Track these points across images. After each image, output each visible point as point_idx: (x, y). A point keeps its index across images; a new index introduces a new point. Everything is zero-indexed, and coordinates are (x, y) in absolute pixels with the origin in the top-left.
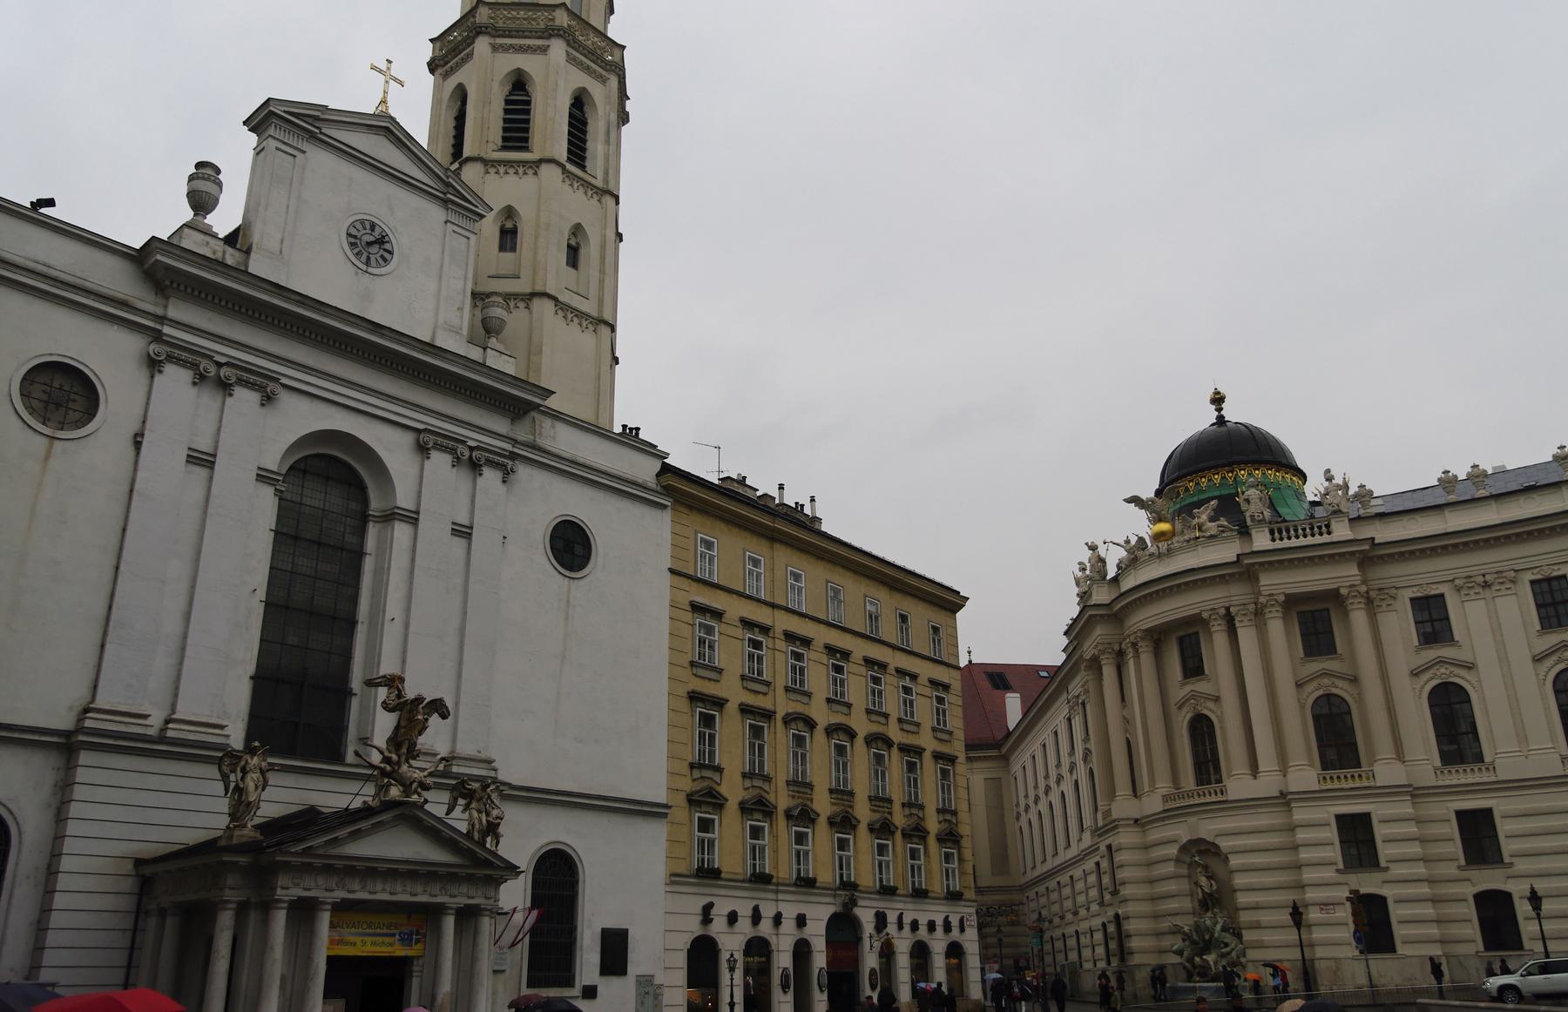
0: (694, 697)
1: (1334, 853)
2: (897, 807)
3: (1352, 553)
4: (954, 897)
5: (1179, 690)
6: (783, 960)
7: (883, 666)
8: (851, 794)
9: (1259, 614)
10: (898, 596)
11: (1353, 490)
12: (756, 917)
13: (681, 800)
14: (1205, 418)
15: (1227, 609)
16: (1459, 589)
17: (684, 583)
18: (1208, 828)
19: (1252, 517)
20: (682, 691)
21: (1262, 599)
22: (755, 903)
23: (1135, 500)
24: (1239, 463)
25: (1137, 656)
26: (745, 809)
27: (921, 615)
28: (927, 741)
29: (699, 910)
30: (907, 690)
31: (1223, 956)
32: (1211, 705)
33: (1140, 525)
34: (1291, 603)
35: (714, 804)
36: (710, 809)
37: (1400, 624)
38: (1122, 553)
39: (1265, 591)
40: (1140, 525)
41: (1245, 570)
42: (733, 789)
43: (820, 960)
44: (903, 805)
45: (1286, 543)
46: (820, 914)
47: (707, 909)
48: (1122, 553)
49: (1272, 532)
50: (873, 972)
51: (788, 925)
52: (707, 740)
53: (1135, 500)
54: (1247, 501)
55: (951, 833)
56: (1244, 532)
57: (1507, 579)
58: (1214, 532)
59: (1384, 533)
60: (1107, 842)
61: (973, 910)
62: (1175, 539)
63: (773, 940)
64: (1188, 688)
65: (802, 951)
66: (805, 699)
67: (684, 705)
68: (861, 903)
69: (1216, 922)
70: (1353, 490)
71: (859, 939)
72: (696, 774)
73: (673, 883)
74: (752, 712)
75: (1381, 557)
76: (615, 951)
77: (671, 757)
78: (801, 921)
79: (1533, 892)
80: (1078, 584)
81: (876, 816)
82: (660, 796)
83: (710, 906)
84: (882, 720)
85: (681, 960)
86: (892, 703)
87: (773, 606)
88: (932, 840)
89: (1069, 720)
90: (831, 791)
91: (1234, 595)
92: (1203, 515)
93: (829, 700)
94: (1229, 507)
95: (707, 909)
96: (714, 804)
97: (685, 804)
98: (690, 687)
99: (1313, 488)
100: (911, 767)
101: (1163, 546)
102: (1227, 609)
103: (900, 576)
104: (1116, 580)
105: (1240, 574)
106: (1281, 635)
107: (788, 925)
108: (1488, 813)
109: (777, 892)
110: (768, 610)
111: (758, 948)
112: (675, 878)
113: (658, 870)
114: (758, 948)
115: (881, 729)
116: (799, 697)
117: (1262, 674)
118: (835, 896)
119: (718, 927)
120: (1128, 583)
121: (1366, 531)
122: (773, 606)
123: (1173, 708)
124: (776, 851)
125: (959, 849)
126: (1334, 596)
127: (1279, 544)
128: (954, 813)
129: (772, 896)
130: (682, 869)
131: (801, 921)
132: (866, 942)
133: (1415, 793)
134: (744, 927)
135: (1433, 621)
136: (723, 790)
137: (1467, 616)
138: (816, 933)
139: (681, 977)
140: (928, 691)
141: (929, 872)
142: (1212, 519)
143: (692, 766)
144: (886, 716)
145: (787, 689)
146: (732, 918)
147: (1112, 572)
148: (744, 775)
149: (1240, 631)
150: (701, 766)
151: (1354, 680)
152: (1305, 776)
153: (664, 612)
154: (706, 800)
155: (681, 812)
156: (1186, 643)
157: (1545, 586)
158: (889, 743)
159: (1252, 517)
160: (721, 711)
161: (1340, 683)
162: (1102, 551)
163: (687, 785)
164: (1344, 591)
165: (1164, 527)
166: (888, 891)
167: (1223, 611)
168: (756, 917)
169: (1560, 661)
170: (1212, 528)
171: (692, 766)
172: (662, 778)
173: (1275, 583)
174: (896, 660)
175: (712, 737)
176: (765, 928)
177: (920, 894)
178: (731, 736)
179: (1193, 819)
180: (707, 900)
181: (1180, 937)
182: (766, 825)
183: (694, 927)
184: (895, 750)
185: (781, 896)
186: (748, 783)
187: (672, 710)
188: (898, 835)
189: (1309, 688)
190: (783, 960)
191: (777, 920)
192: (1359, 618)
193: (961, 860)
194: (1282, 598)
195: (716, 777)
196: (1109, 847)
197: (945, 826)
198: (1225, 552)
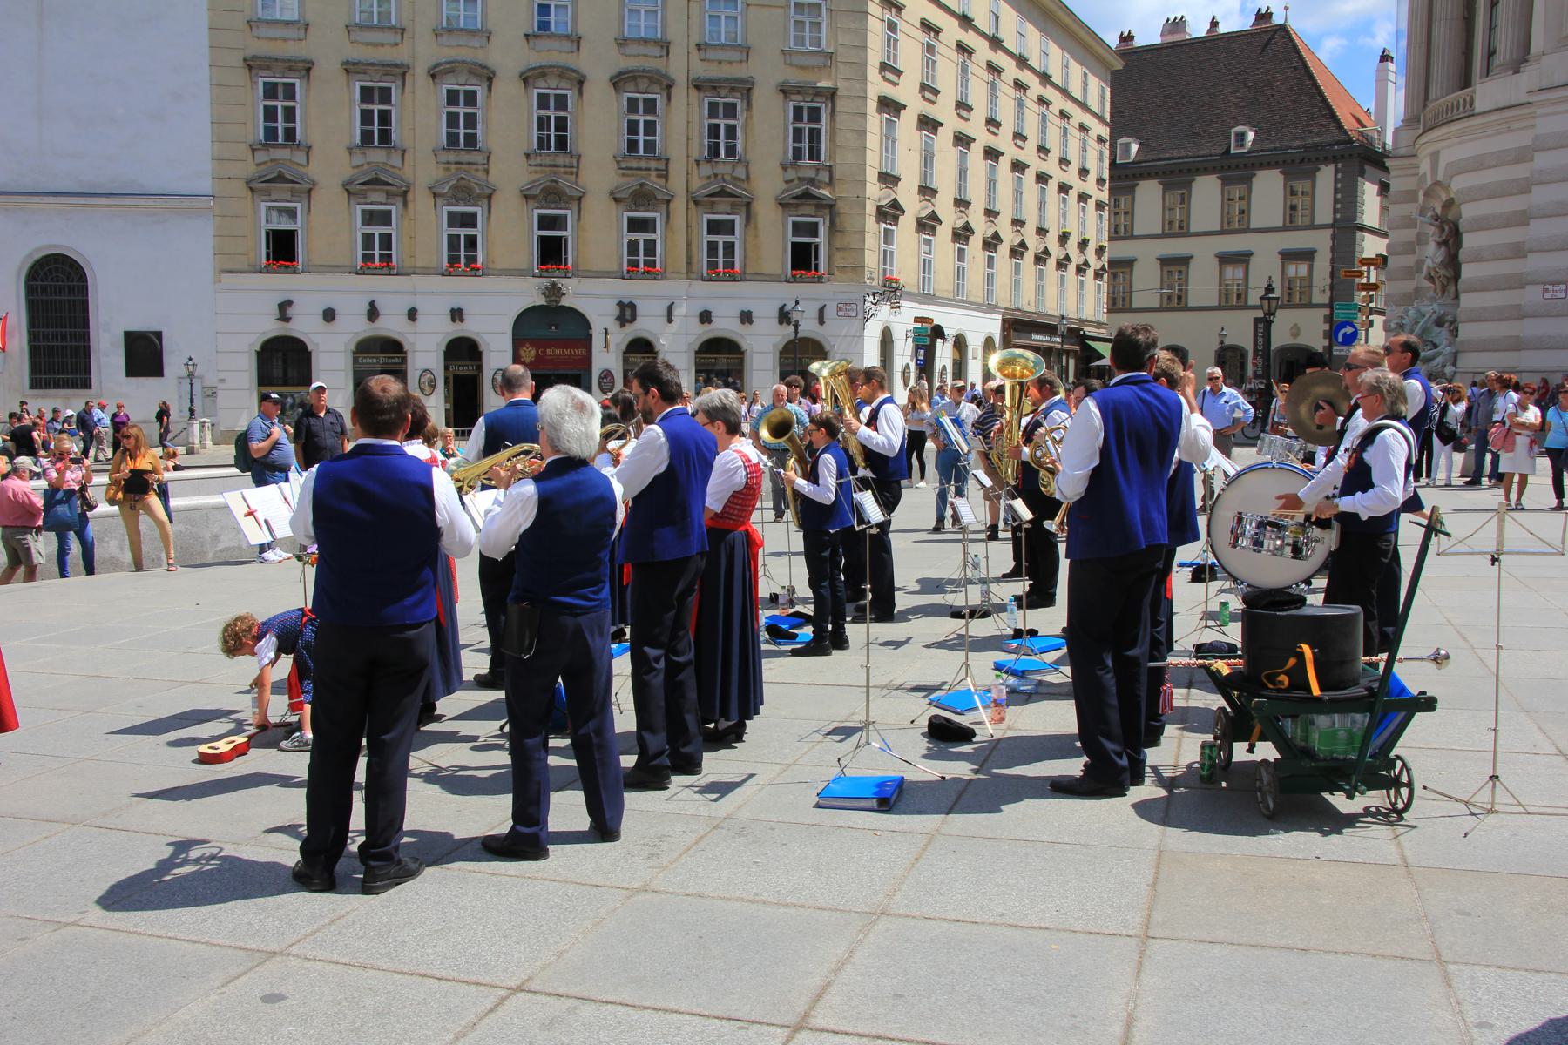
0: (252, 65)
12: (373, 313)
13: (240, 188)
20: (236, 59)
29: (276, 310)
65: (463, 352)
72: (262, 156)
77: (218, 139)
83: (290, 303)
98: (250, 53)
119: (305, 326)
134: (353, 327)
136: (315, 170)
145: (437, 33)
146: (329, 315)
150: (265, 146)
163: (249, 169)
168: (373, 313)
176: (391, 325)
183: (271, 327)
187: (217, 85)
190: (426, 355)
193: (833, 228)
195: (300, 157)
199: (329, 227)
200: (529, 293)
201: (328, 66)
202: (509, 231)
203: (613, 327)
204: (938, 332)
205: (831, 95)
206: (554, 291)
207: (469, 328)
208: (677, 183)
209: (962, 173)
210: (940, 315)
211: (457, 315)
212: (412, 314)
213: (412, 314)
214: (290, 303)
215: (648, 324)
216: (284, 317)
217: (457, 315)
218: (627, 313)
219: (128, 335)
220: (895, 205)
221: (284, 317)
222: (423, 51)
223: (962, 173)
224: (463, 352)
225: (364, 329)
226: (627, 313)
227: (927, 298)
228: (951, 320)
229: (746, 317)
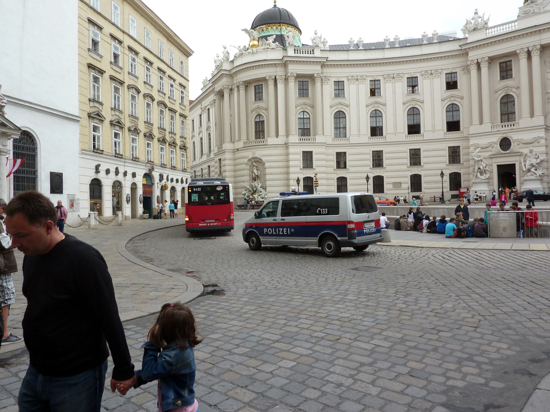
0: (90, 66)
1: (300, 163)
2: (167, 133)
3: (320, 62)
4: (184, 170)
5: (253, 105)
6: (127, 191)
7: (164, 73)
8: (152, 125)
9: (286, 79)
10: (170, 44)
11: (322, 40)
14: (270, 6)
15: (275, 77)
16: (348, 80)
18: (259, 153)
19: (289, 43)
20: (85, 62)
21: (289, 74)
22: (117, 166)
23: (245, 30)
24: (283, 23)
25: (238, 90)
26: (112, 124)
27: (177, 55)
28: (177, 107)
30: (172, 86)
31: (260, 195)
32: (264, 111)
33: (245, 40)
34: (298, 76)
35: (100, 120)
36: (98, 122)
37: (329, 89)
38: (237, 51)
39: (290, 71)
40: (245, 40)
41: (284, 64)
43: (140, 191)
44: (169, 133)
45: (299, 55)
46: (141, 172)
47: (97, 167)
48: (237, 51)
49: (295, 50)
50: (158, 196)
51: (129, 176)
52: (96, 89)
53: (245, 30)
54: (288, 37)
55: (184, 146)
56: (285, 49)
57: (363, 78)
58: (274, 47)
59: (333, 56)
60: (219, 158)
61: (190, 176)
62: (259, 48)
63: (123, 182)
64: (256, 105)
65: (134, 187)
66: (136, 80)
68: (155, 170)
69: (258, 184)
70: (322, 40)
71: (153, 184)
72: (92, 104)
73: (83, 153)
74: (115, 80)
75: (327, 65)
77: (81, 94)
78: (134, 175)
79: (367, 176)
80: (215, 62)
81: (161, 136)
82: (76, 112)
83: (99, 165)
84: (163, 96)
85: (87, 189)
86: (167, 90)
87: (124, 32)
88: (178, 147)
89: (200, 115)
90: (145, 122)
91: (279, 72)
92: (271, 40)
93: (145, 82)
94: (280, 39)
95: (97, 167)
96: (100, 120)
97: (87, 118)
99: (306, 39)
100: (172, 118)
101: (255, 49)
102: (275, 77)
103: (172, 35)
104: (232, 62)
105: (282, 64)
106: (293, 86)
107: (129, 176)
108: (345, 153)
109: (125, 162)
110: (121, 33)
111: (117, 186)
112: (83, 151)
114: (117, 186)
115: (163, 100)
116: (133, 78)
117: (284, 101)
118: (146, 166)
119: (102, 176)
120: (237, 63)
121: (325, 55)
122: (124, 32)
123: (250, 111)
124: (124, 145)
125: (186, 152)
126: (312, 77)
127: (296, 55)
128: (185, 138)
129: (123, 164)
131: (134, 175)
132: (156, 185)
133: (327, 146)
134: (112, 177)
135: (339, 88)
136: (103, 113)
137: (350, 89)
138: (140, 181)
139: (87, 195)
140: (178, 87)
141: (176, 160)
142: (273, 42)
143: (90, 100)
144: (165, 94)
146: (108, 172)
147: (231, 58)
148: (112, 109)
149: (278, 85)
150: (94, 101)
151: (313, 107)
152: (294, 138)
153: (76, 20)
154: (96, 116)
155: (85, 120)
156: (257, 87)
157: (373, 82)
158: (166, 106)
159: (289, 43)
160: (102, 77)
161: (308, 107)
162: (228, 49)
163: (88, 108)
164: (315, 75)
165: (256, 43)
166: (163, 166)
167: (274, 77)
168: (117, 172)
169: (374, 107)
170: (273, 45)
171: (90, 100)
172: (76, 104)
173: (294, 69)
174: (169, 72)
175: (98, 88)
176: (120, 177)
177: (173, 168)
178: (106, 88)
179: (253, 150)
180: (97, 163)
181: (244, 189)
182: (120, 133)
184: (167, 109)
185: (126, 164)
186: (113, 113)
188: (167, 144)
189: (298, 108)
190: (127, 191)
191: (125, 174)
192: (318, 84)
193: (187, 157)
194: (295, 75)
195: (100, 107)
196: (220, 160)
197: (182, 143)
198: (277, 54)
214: (99, 165)
219: (52, 175)
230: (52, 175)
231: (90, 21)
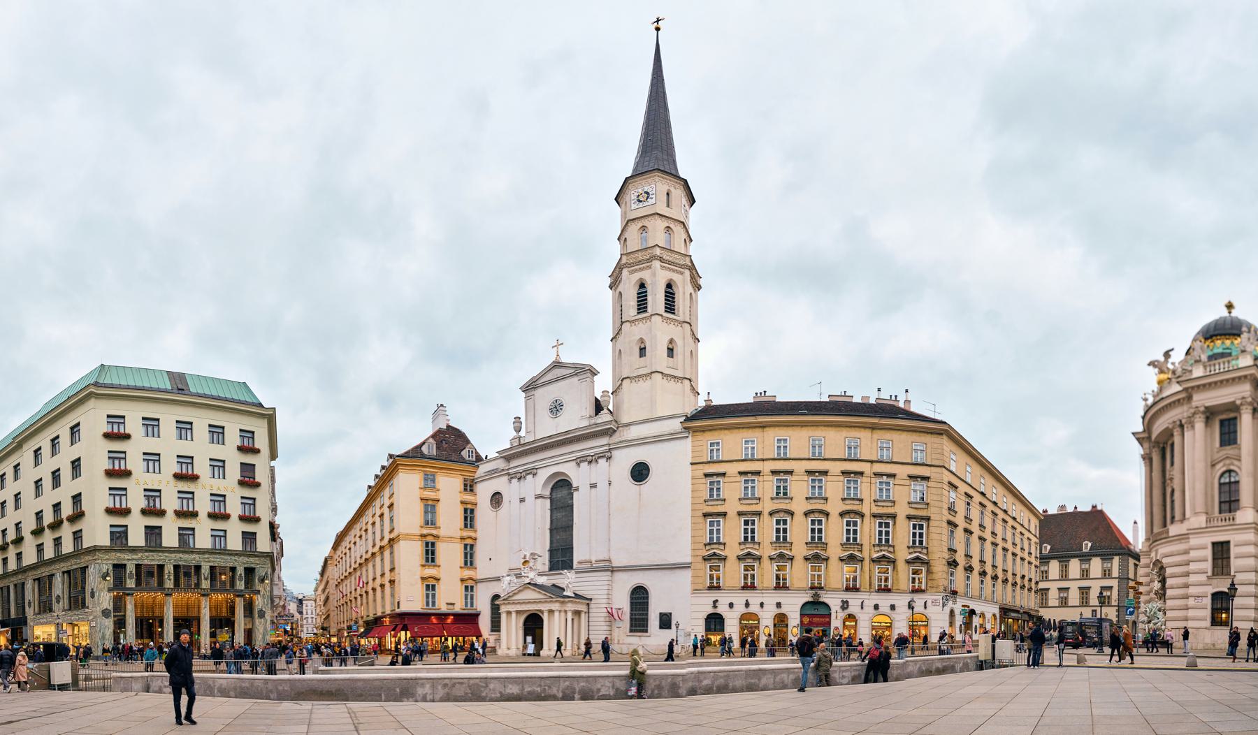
0: (706, 515)
12: (747, 605)
17: (700, 466)
42: (732, 550)
63: (761, 614)
65: (781, 620)
67: (701, 519)
76: (665, 621)
77: (694, 543)
82: (688, 560)
113: (689, 588)
119: (722, 609)
130: (700, 587)
132: (833, 616)
134: (740, 609)
146: (731, 605)
154: (714, 559)
168: (747, 605)
172: (690, 552)
176: (754, 608)
183: (710, 610)
199: (732, 573)
200: (807, 597)
201: (732, 513)
202: (799, 574)
203: (840, 610)
204: (972, 612)
205: (928, 519)
206: (816, 595)
207: (783, 610)
208: (866, 554)
209: (982, 551)
210: (973, 605)
211: (779, 605)
212: (762, 605)
213: (762, 605)
215: (854, 609)
216: (715, 607)
217: (779, 605)
218: (845, 604)
219: (662, 615)
220: (955, 561)
221: (715, 607)
222: (767, 506)
223: (982, 551)
224: (781, 620)
225: (744, 610)
226: (845, 604)
227: (966, 595)
228: (978, 607)
229: (893, 607)
230: (662, 615)
231: (706, 475)
